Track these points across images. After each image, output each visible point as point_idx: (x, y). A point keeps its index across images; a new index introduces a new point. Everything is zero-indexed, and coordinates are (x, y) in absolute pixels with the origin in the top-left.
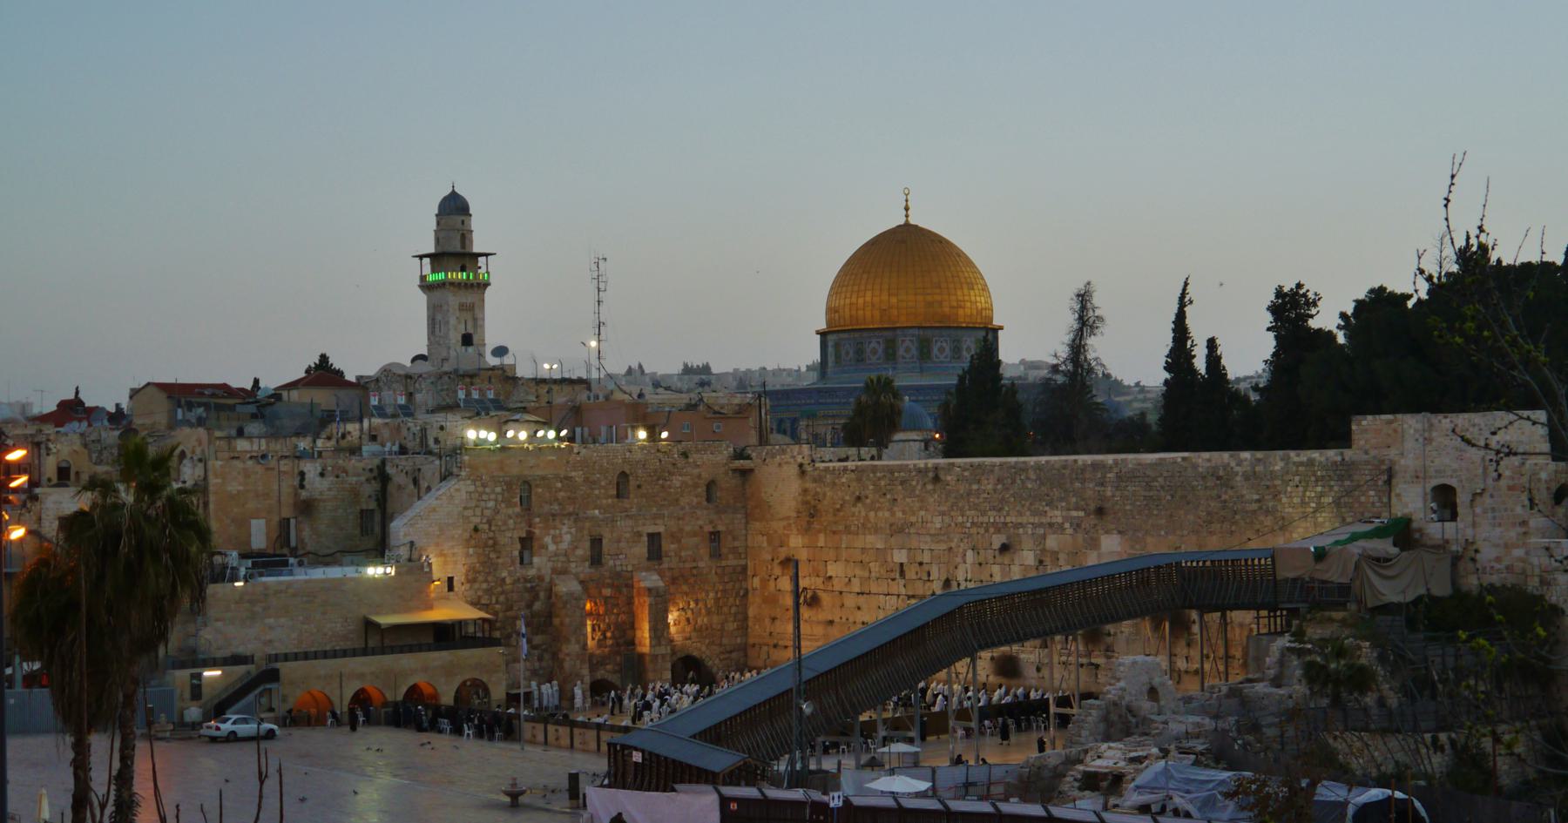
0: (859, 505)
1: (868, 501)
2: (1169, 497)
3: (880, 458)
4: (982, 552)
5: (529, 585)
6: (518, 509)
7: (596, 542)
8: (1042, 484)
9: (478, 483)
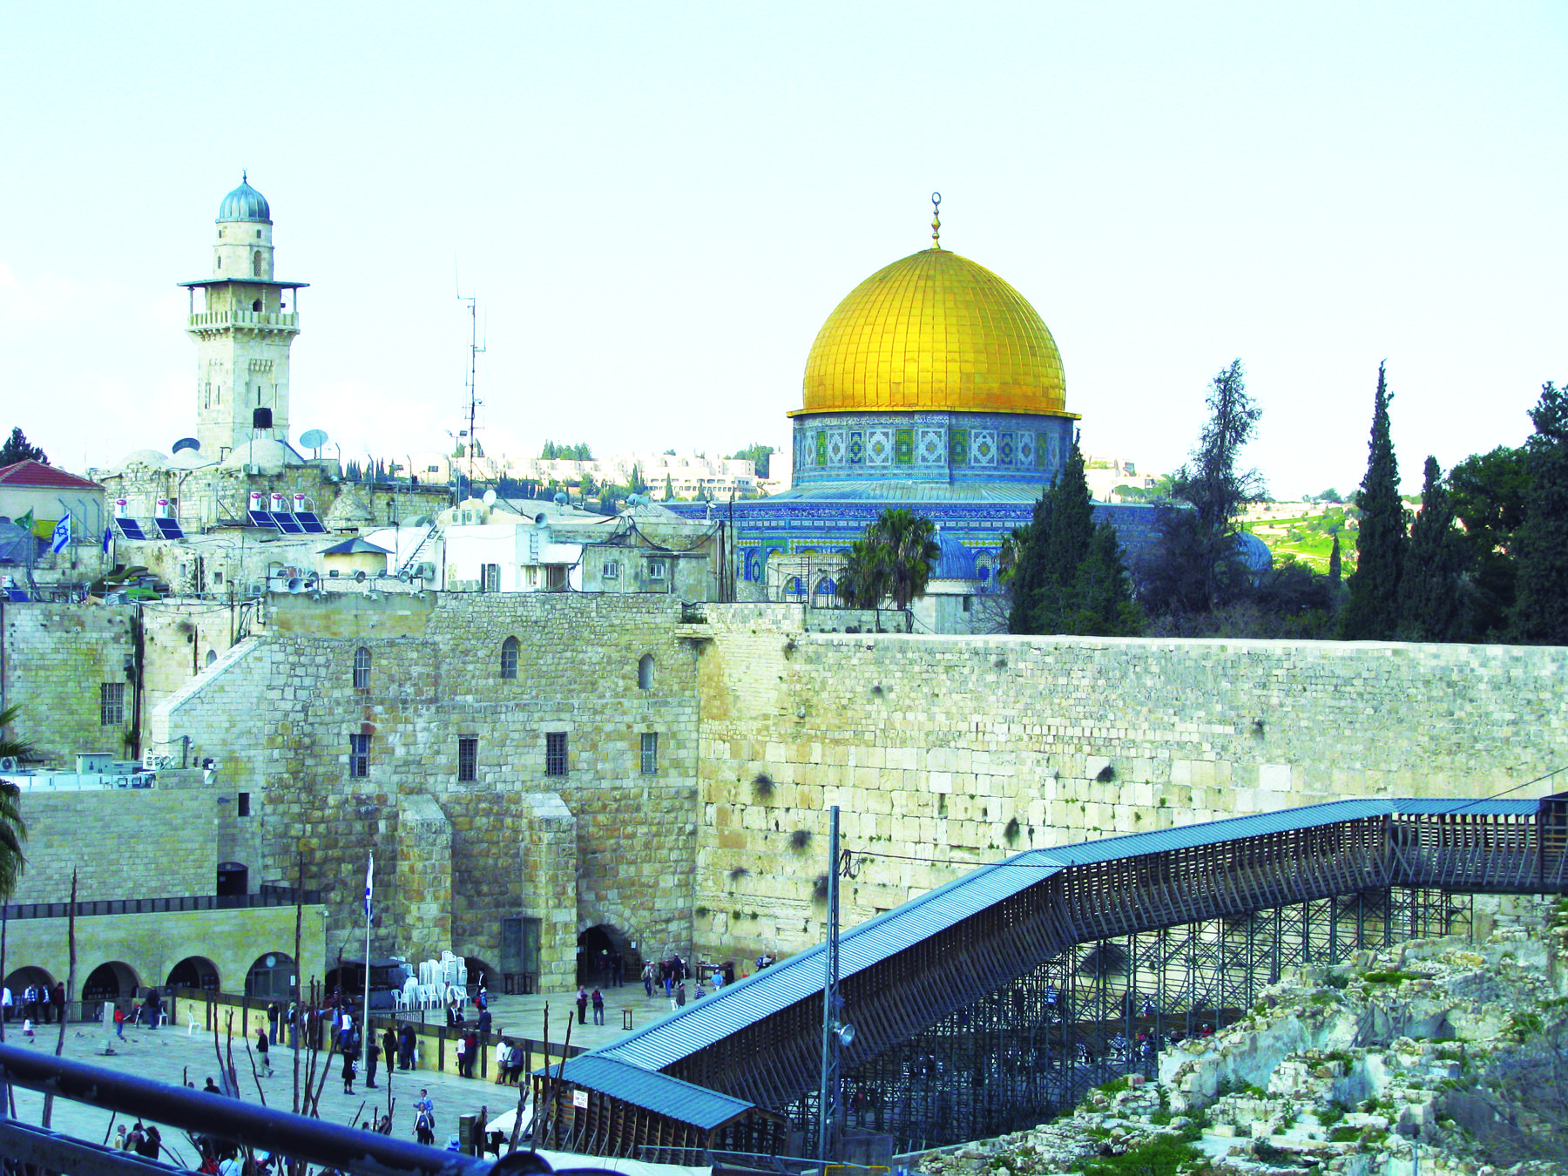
1: (892, 696)
2: (1370, 711)
3: (910, 630)
4: (1070, 782)
5: (363, 809)
6: (349, 691)
7: (468, 746)
8: (1168, 681)
9: (290, 649)
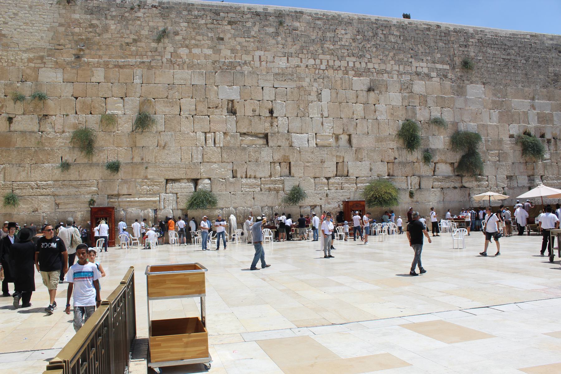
0: (166, 41)
1: (177, 38)
